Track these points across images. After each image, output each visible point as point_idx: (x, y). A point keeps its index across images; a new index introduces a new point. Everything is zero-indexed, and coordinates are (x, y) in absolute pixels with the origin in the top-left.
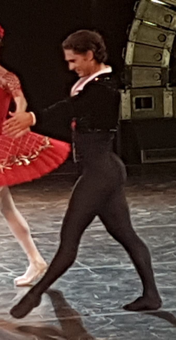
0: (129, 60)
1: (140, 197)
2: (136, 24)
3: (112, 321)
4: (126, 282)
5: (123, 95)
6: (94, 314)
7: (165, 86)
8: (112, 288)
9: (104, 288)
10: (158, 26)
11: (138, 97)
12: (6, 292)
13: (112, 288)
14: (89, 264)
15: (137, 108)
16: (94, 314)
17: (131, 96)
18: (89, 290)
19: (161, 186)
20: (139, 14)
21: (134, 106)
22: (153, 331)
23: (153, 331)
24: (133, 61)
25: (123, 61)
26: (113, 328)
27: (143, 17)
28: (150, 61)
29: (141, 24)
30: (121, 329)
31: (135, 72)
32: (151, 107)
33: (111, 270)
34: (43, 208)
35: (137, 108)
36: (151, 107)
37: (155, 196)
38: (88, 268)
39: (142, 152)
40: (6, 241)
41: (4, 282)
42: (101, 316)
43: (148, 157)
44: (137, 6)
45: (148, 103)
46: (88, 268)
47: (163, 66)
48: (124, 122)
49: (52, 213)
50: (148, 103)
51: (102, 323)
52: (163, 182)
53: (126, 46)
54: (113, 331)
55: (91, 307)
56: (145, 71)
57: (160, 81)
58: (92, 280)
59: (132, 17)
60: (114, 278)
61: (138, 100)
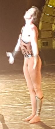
7: (53, 38)
10: (51, 15)
11: (43, 41)
15: (43, 45)
17: (41, 41)
19: (52, 74)
20: (44, 11)
21: (42, 45)
24: (42, 28)
27: (45, 12)
28: (48, 28)
29: (45, 14)
34: (9, 82)
35: (43, 45)
36: (48, 45)
44: (43, 8)
47: (52, 30)
49: (12, 84)
52: (51, 73)
57: (51, 36)
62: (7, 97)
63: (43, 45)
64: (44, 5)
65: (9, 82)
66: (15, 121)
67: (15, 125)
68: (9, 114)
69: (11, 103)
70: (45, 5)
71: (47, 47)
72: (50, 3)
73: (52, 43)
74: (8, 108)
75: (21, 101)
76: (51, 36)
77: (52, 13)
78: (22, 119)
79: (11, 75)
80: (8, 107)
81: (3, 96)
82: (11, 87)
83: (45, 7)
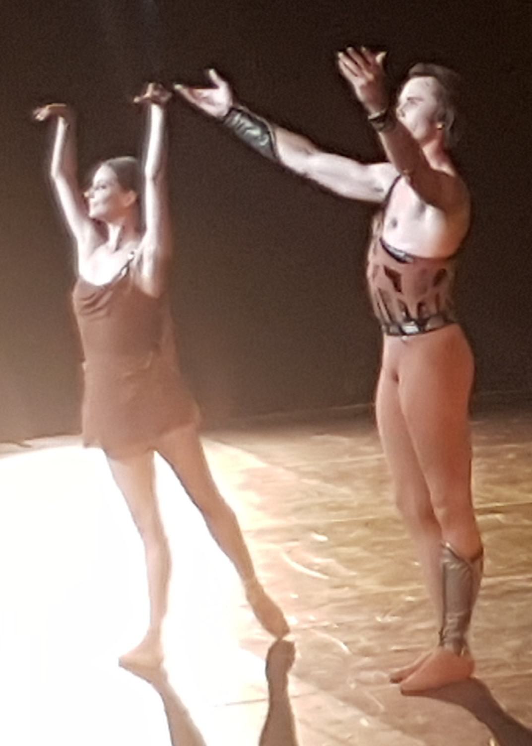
34: (511, 456)
62: (499, 532)
65: (511, 456)
68: (513, 624)
69: (522, 568)
74: (509, 592)
79: (515, 421)
80: (506, 588)
82: (521, 481)
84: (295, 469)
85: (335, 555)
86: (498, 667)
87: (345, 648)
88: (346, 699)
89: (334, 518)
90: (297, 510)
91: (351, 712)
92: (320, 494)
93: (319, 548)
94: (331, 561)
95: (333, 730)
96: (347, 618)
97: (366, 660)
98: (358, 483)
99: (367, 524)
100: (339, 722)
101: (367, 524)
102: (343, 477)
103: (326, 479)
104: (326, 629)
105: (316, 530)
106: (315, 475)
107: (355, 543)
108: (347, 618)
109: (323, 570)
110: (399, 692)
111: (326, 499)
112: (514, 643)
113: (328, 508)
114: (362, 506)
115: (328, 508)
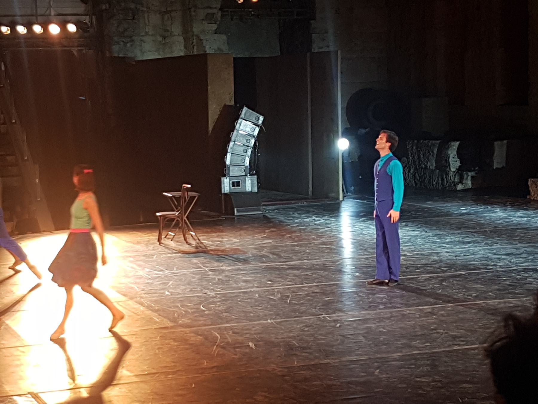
0: (228, 162)
1: (234, 232)
2: (231, 144)
3: (218, 296)
4: (226, 276)
5: (225, 180)
6: (209, 293)
8: (219, 279)
9: (214, 279)
12: (164, 282)
13: (219, 279)
14: (207, 267)
16: (209, 293)
17: (230, 181)
18: (206, 280)
19: (245, 227)
20: (233, 139)
22: (239, 301)
23: (239, 301)
25: (225, 162)
26: (218, 300)
30: (223, 300)
31: (231, 168)
32: (240, 186)
33: (218, 270)
36: (240, 186)
37: (242, 232)
38: (207, 269)
39: (235, 209)
40: (164, 255)
41: (163, 276)
42: (213, 294)
43: (238, 211)
45: (238, 184)
46: (207, 269)
48: (226, 194)
50: (238, 184)
51: (213, 297)
52: (245, 225)
53: (226, 155)
54: (219, 301)
55: (208, 289)
56: (236, 168)
58: (208, 275)
59: (229, 140)
60: (220, 274)
61: (233, 183)
63: (233, 186)
64: (233, 131)
66: (192, 293)
67: (192, 299)
70: (235, 131)
71: (237, 189)
72: (241, 128)
73: (245, 183)
75: (200, 265)
76: (244, 174)
77: (245, 141)
78: (202, 290)
81: (175, 258)
83: (235, 132)
84: (125, 241)
85: (135, 264)
86: (178, 295)
87: (137, 289)
88: (136, 302)
89: (135, 254)
90: (127, 251)
91: (138, 306)
92: (132, 247)
93: (131, 262)
94: (135, 266)
95: (133, 310)
96: (138, 281)
97: (143, 292)
98: (143, 245)
99: (144, 256)
100: (135, 308)
101: (144, 256)
102: (138, 243)
103: (134, 243)
104: (132, 283)
105: (130, 257)
106: (130, 242)
107: (141, 261)
108: (138, 281)
109: (132, 268)
110: (106, 265)
111: (133, 249)
112: (183, 287)
113: (133, 251)
114: (143, 251)
115: (133, 251)
